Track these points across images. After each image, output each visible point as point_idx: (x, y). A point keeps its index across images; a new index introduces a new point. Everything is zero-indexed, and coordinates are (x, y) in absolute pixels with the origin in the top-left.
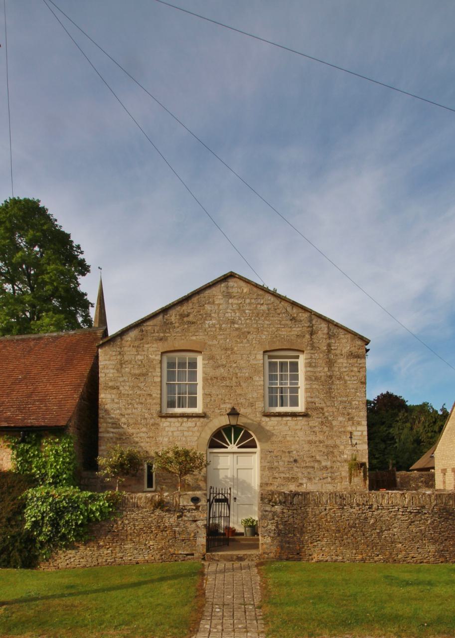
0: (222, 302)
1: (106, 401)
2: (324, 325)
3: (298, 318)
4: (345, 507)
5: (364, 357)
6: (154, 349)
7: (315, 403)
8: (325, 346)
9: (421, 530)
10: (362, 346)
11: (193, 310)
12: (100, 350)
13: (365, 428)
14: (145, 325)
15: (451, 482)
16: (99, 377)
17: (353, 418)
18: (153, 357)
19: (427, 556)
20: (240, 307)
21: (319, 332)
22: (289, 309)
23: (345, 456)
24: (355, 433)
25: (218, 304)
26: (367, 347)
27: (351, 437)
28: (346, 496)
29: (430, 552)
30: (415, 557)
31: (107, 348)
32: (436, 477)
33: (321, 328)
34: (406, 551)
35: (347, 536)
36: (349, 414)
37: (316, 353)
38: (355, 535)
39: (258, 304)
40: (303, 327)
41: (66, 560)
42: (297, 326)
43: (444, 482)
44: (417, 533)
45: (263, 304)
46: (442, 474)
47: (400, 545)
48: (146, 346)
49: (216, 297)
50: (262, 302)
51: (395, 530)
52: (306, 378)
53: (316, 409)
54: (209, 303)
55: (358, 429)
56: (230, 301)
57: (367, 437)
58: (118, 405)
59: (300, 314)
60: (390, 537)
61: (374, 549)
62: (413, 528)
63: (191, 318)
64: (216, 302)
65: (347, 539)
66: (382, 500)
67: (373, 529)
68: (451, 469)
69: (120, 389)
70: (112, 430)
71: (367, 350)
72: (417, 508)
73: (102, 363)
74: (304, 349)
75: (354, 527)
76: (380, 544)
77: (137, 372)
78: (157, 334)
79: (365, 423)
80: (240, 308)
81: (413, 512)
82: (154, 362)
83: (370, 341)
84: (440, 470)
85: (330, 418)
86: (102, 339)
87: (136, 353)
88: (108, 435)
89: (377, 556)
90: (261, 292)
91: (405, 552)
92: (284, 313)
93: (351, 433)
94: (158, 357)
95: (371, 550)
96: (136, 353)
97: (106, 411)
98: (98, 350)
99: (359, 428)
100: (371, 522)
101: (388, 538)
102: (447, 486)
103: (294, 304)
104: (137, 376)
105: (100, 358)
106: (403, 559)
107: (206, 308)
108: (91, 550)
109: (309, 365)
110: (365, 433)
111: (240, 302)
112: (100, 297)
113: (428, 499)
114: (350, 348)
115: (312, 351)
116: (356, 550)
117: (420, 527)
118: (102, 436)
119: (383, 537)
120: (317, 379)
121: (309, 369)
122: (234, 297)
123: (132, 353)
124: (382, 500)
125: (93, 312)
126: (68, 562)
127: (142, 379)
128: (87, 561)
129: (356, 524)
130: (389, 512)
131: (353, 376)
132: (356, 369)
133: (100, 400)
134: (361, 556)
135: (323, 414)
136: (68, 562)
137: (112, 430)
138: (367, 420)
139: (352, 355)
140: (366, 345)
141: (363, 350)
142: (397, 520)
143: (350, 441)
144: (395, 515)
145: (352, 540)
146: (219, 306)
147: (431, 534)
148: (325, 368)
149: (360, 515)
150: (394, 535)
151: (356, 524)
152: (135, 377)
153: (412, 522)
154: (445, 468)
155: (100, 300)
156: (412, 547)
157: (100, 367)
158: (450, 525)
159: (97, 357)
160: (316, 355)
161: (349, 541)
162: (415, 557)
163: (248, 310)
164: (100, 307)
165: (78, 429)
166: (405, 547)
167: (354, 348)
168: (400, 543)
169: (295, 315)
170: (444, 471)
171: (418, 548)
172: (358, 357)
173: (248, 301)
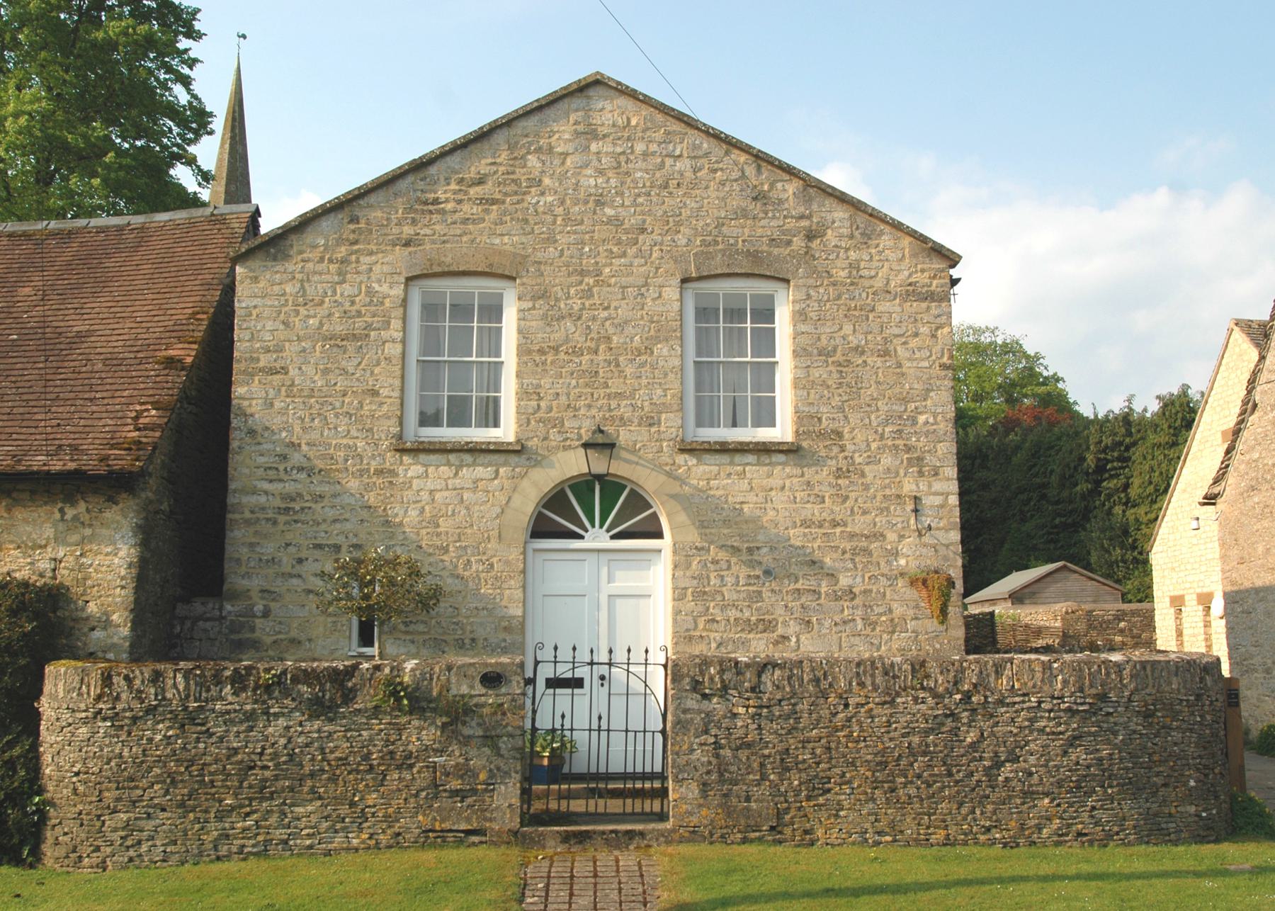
0: (570, 148)
1: (250, 405)
2: (840, 214)
3: (773, 194)
4: (899, 700)
5: (945, 298)
6: (386, 269)
7: (820, 419)
8: (843, 269)
9: (1101, 759)
10: (942, 271)
11: (495, 168)
12: (238, 269)
13: (954, 487)
14: (361, 202)
15: (1196, 631)
16: (233, 341)
17: (920, 459)
18: (384, 288)
19: (1116, 829)
20: (619, 163)
21: (829, 232)
22: (750, 171)
23: (902, 562)
24: (928, 501)
25: (561, 154)
26: (955, 273)
27: (916, 511)
28: (900, 669)
29: (1124, 819)
30: (1086, 835)
31: (255, 263)
32: (1157, 618)
33: (833, 222)
34: (1061, 818)
35: (906, 777)
36: (908, 449)
37: (821, 285)
38: (925, 774)
39: (668, 156)
40: (785, 217)
41: (128, 847)
42: (770, 215)
43: (1180, 634)
44: (1088, 767)
45: (679, 156)
46: (1172, 610)
47: (1047, 801)
48: (366, 260)
49: (557, 136)
50: (677, 153)
51: (1032, 760)
52: (794, 351)
53: (821, 435)
54: (539, 150)
55: (933, 490)
56: (594, 147)
57: (958, 509)
58: (285, 419)
59: (779, 185)
60: (1019, 780)
61: (978, 812)
62: (1078, 754)
63: (487, 189)
64: (559, 150)
65: (905, 787)
66: (997, 679)
67: (974, 759)
68: (1194, 597)
69: (291, 373)
70: (266, 486)
71: (954, 282)
72: (1087, 700)
73: (242, 302)
74: (789, 276)
75: (925, 754)
76: (993, 798)
77: (339, 328)
78: (395, 230)
79: (952, 472)
80: (620, 165)
81: (1078, 711)
82: (387, 303)
83: (960, 257)
84: (1168, 600)
85: (858, 460)
86: (244, 239)
87: (336, 278)
88: (253, 500)
89: (984, 833)
90: (676, 127)
91: (1058, 821)
92: (736, 180)
93: (916, 498)
94: (398, 291)
95: (970, 817)
96: (336, 278)
97: (252, 432)
98: (233, 270)
99: (937, 486)
100: (969, 740)
101: (1014, 783)
102: (1186, 644)
103: (760, 158)
104: (338, 341)
105: (240, 289)
106: (1055, 838)
107: (529, 164)
108: (197, 820)
109: (800, 316)
110: (954, 500)
111: (619, 150)
112: (234, 112)
113: (1113, 676)
114: (910, 275)
115: (811, 282)
116: (929, 815)
117: (1098, 750)
118: (236, 501)
119: (1000, 778)
120: (825, 353)
121: (803, 328)
122: (605, 136)
123: (328, 278)
124: (997, 679)
125: (208, 151)
126: (132, 853)
127: (351, 346)
128: (187, 851)
129: (927, 746)
130: (1016, 712)
131: (920, 349)
132: (924, 330)
133: (234, 402)
134: (943, 833)
135: (843, 449)
136: (132, 853)
137: (266, 486)
138: (959, 465)
139: (912, 293)
140: (953, 266)
141: (942, 281)
142: (1035, 734)
143: (912, 521)
144: (1029, 720)
145: (918, 788)
146: (565, 159)
147: (1127, 769)
148: (845, 327)
149: (938, 720)
150: (1030, 774)
151: (927, 746)
152: (332, 342)
153: (1075, 738)
154: (1181, 593)
155: (234, 119)
156: (1077, 805)
157: (238, 312)
158: (1176, 744)
159: (229, 290)
160: (821, 290)
161: (913, 791)
162: (1086, 835)
163: (641, 170)
164: (233, 138)
165: (436, 594)
166: (1059, 805)
167: (919, 274)
168: (1047, 794)
169: (766, 187)
170: (1178, 603)
171: (1094, 808)
172: (930, 297)
173: (640, 147)
